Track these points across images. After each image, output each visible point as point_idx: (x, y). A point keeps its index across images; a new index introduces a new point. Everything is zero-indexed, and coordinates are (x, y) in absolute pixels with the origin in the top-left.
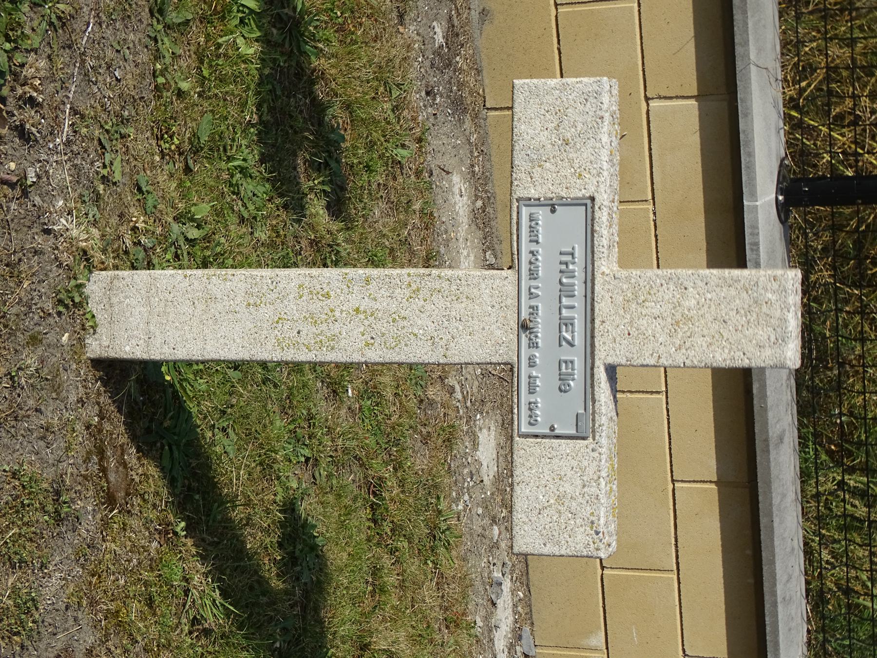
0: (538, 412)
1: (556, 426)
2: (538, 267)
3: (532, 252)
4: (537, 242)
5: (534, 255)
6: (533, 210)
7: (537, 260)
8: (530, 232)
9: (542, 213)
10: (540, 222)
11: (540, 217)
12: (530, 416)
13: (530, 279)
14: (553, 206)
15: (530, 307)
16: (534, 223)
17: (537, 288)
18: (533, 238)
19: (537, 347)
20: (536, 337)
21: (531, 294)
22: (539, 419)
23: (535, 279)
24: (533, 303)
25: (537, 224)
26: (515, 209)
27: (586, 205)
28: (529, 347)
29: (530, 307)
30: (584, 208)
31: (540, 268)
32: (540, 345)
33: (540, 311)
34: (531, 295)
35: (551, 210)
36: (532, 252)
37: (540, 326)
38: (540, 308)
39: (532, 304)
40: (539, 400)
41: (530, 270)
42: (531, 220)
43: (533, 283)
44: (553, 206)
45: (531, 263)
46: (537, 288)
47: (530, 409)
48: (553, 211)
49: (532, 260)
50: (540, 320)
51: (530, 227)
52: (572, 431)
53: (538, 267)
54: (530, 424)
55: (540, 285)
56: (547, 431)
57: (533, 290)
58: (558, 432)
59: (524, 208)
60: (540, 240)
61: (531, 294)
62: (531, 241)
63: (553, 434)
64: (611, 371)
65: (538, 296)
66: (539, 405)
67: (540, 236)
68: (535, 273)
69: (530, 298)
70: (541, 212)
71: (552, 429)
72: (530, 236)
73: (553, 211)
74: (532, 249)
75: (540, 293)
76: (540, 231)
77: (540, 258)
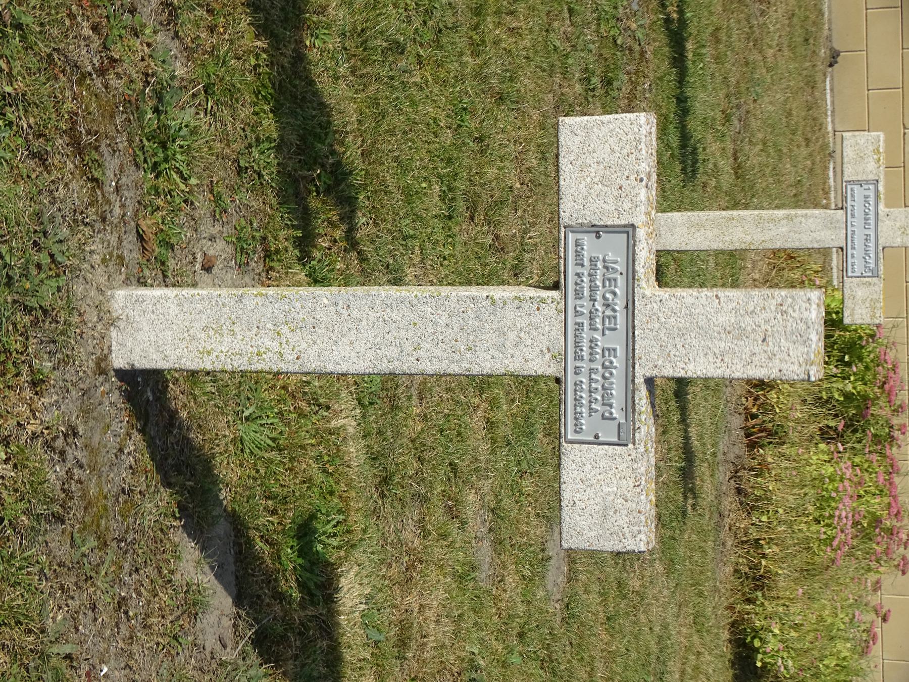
3: (578, 275)
4: (583, 265)
7: (582, 281)
13: (576, 298)
14: (598, 232)
17: (582, 306)
19: (582, 360)
20: (582, 350)
21: (576, 311)
23: (581, 298)
24: (579, 320)
26: (562, 235)
28: (575, 359)
29: (576, 324)
32: (585, 358)
34: (577, 313)
36: (578, 275)
37: (585, 341)
38: (585, 324)
39: (578, 320)
41: (576, 290)
43: (579, 302)
45: (576, 284)
46: (582, 306)
50: (585, 336)
53: (583, 287)
55: (585, 304)
57: (578, 309)
59: (571, 236)
60: (585, 264)
61: (576, 311)
62: (576, 264)
65: (583, 313)
67: (585, 259)
69: (576, 316)
72: (576, 260)
74: (578, 271)
75: (585, 311)
77: (585, 279)
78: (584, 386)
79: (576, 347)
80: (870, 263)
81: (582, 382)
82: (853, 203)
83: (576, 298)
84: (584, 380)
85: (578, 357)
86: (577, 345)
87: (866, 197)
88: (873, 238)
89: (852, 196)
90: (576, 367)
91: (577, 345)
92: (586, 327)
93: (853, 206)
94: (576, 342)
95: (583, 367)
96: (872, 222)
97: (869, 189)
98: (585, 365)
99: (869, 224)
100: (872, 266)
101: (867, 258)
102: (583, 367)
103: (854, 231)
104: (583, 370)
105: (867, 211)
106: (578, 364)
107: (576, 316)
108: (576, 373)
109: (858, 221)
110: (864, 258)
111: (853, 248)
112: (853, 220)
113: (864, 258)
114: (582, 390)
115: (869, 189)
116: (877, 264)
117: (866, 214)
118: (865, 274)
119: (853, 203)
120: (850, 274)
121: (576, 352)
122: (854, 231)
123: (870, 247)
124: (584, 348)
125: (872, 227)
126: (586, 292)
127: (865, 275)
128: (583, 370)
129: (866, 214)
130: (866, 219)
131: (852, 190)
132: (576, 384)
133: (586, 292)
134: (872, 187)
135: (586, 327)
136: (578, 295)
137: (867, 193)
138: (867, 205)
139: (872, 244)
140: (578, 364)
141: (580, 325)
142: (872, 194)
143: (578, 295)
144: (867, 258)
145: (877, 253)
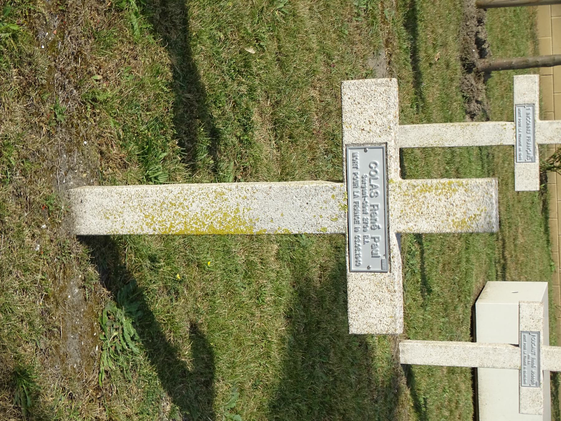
0: (360, 259)
1: (370, 266)
2: (358, 181)
3: (354, 174)
4: (357, 168)
5: (355, 175)
6: (354, 151)
7: (357, 177)
8: (353, 163)
9: (359, 153)
10: (358, 158)
11: (358, 155)
12: (356, 262)
13: (354, 188)
14: (365, 149)
15: (354, 202)
16: (354, 158)
17: (358, 192)
18: (354, 166)
19: (359, 223)
20: (358, 218)
22: (361, 263)
23: (357, 187)
24: (356, 200)
25: (357, 159)
27: (383, 148)
28: (355, 223)
30: (382, 149)
31: (359, 182)
32: (360, 222)
33: (360, 204)
35: (365, 151)
36: (354, 174)
37: (360, 212)
40: (361, 253)
41: (354, 183)
42: (353, 157)
43: (355, 190)
44: (365, 149)
45: (354, 179)
46: (358, 192)
47: (356, 258)
48: (366, 151)
49: (355, 178)
50: (359, 209)
51: (353, 160)
52: (380, 269)
53: (358, 181)
54: (356, 265)
56: (366, 269)
57: (355, 194)
58: (371, 269)
60: (359, 167)
62: (353, 168)
63: (369, 270)
64: (399, 235)
65: (358, 196)
66: (361, 256)
67: (358, 165)
68: (356, 184)
69: (354, 198)
70: (358, 152)
71: (368, 267)
72: (353, 165)
73: (366, 151)
74: (355, 172)
75: (359, 195)
76: (359, 162)
77: (358, 176)
78: (360, 239)
79: (355, 216)
80: (530, 154)
81: (359, 236)
82: (520, 118)
83: (354, 188)
84: (360, 235)
85: (357, 222)
86: (355, 215)
87: (528, 114)
88: (532, 139)
89: (519, 113)
90: (355, 228)
91: (355, 215)
92: (360, 205)
93: (519, 120)
94: (355, 213)
95: (359, 228)
96: (531, 129)
97: (529, 109)
98: (360, 226)
99: (530, 130)
100: (532, 155)
101: (528, 151)
102: (359, 228)
103: (520, 135)
104: (359, 229)
105: (528, 122)
106: (357, 226)
107: (354, 198)
108: (355, 231)
109: (523, 129)
110: (527, 151)
111: (520, 145)
112: (520, 128)
113: (527, 151)
114: (359, 241)
115: (529, 109)
116: (534, 153)
117: (528, 124)
118: (527, 161)
119: (520, 118)
120: (518, 161)
121: (355, 219)
122: (520, 135)
123: (530, 144)
124: (360, 217)
125: (531, 132)
126: (360, 184)
127: (527, 161)
128: (359, 229)
129: (528, 124)
130: (528, 128)
131: (519, 110)
132: (355, 238)
133: (360, 184)
134: (531, 108)
135: (360, 205)
136: (355, 185)
137: (528, 112)
138: (528, 119)
139: (531, 143)
140: (357, 226)
141: (357, 203)
142: (531, 112)
143: (355, 185)
144: (528, 151)
145: (534, 148)
